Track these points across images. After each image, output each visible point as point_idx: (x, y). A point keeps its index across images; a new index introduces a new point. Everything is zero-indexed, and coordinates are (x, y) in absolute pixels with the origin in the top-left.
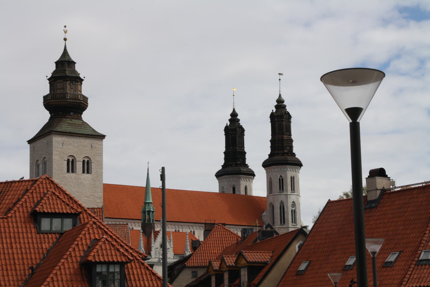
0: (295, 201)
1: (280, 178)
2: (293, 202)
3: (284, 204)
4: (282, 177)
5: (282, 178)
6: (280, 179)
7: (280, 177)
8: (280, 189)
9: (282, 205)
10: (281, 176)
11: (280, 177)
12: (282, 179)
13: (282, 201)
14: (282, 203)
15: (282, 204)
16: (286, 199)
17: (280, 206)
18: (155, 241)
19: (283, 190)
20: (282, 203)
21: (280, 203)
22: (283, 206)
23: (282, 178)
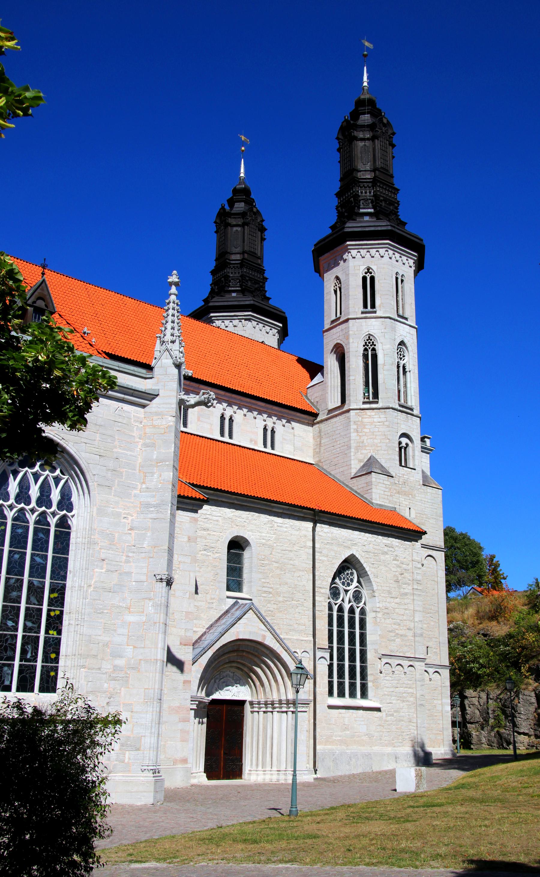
0: (406, 341)
1: (367, 275)
2: (399, 344)
3: (375, 345)
4: (371, 273)
5: (370, 275)
6: (364, 279)
7: (366, 273)
8: (365, 306)
9: (371, 347)
10: (368, 269)
11: (366, 273)
12: (372, 279)
13: (369, 337)
14: (369, 343)
15: (371, 346)
16: (383, 331)
17: (366, 350)
19: (373, 306)
20: (369, 343)
21: (366, 343)
22: (374, 350)
23: (370, 275)
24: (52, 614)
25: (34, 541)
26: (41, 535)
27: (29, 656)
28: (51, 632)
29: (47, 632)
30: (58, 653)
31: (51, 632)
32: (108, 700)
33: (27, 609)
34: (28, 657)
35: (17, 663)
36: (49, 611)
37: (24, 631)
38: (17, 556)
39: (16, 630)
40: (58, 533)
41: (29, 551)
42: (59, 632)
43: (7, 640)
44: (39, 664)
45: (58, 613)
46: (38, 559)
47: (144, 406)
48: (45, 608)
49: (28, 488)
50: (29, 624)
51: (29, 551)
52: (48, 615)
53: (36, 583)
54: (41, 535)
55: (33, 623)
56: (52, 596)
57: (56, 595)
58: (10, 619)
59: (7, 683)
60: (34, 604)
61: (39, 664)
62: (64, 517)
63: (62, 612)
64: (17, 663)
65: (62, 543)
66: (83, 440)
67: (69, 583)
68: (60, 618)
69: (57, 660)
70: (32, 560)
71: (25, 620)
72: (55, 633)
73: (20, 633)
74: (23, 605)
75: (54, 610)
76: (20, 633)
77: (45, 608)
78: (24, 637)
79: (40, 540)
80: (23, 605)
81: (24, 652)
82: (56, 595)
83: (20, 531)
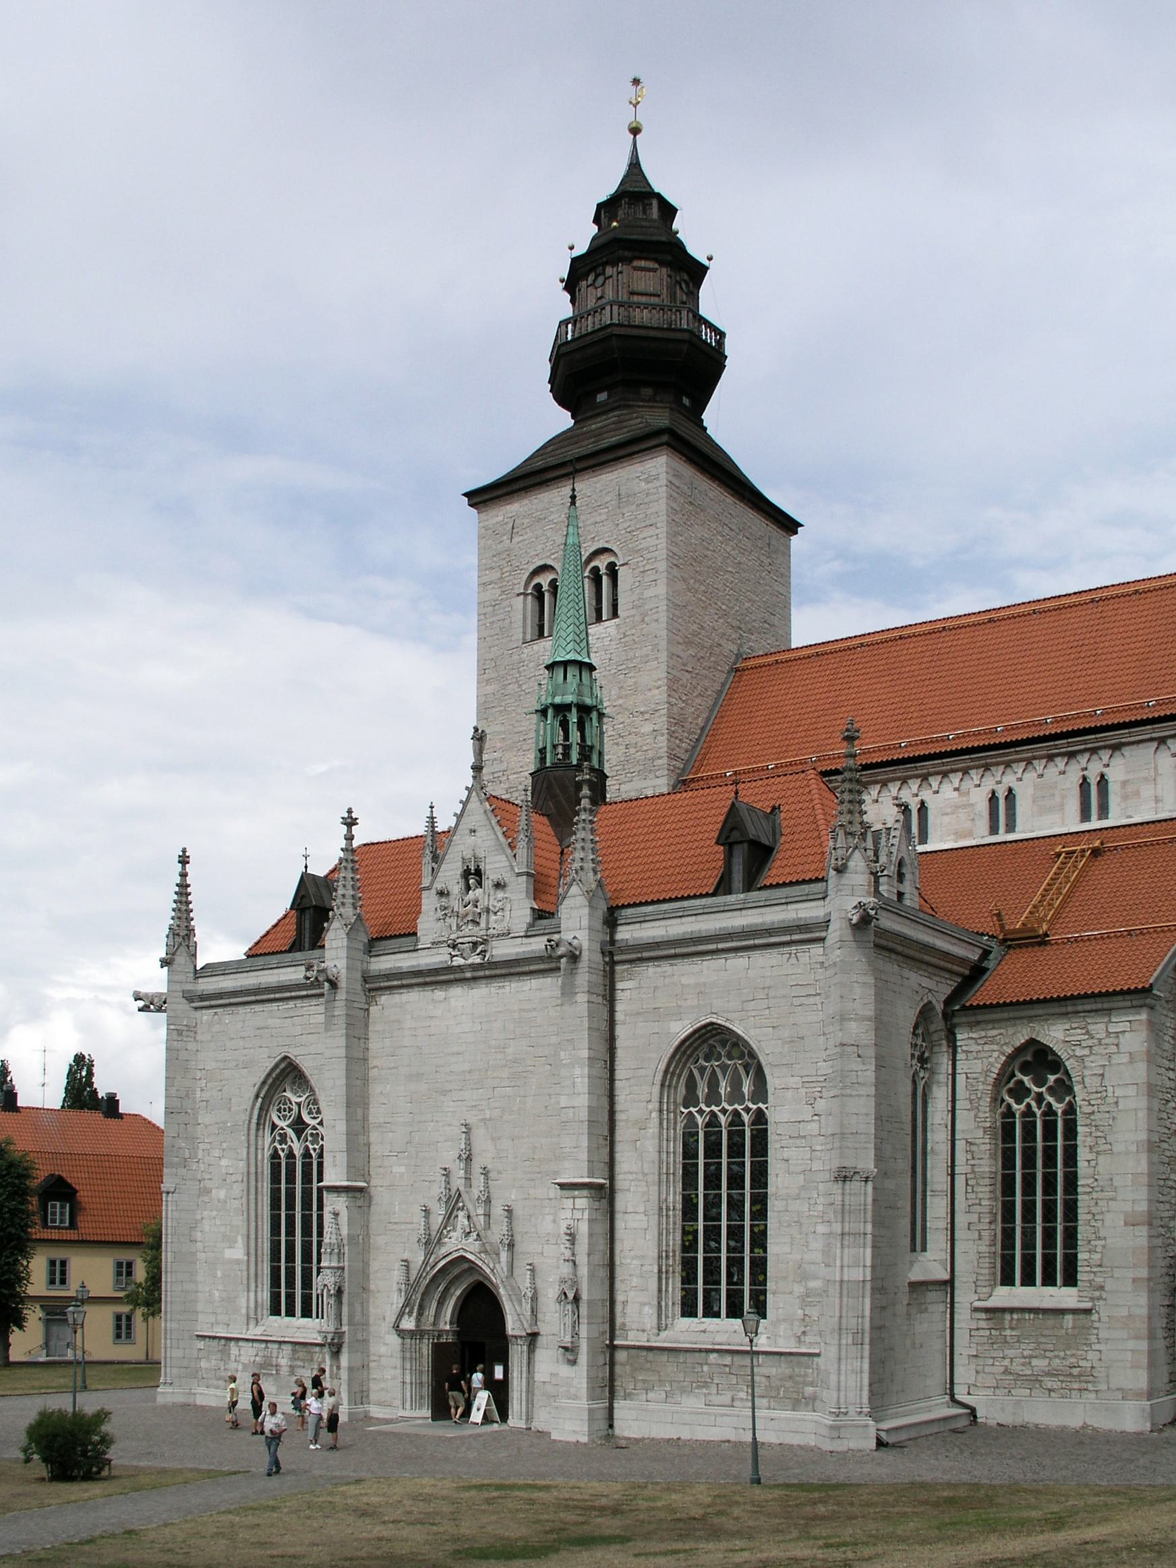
18: (435, 858)
24: (756, 1230)
25: (729, 1147)
26: (736, 1139)
27: (735, 1279)
28: (756, 1250)
29: (752, 1251)
30: (766, 1275)
31: (756, 1250)
32: (803, 1329)
33: (729, 1226)
34: (735, 1280)
35: (724, 1287)
36: (752, 1226)
37: (728, 1252)
38: (712, 1168)
39: (720, 1251)
40: (755, 1132)
41: (724, 1160)
42: (765, 1251)
43: (712, 1263)
44: (747, 1288)
45: (762, 1228)
46: (735, 1167)
47: (823, 939)
48: (747, 1223)
49: (718, 1085)
50: (732, 1243)
51: (724, 1160)
52: (752, 1231)
53: (735, 1196)
54: (736, 1139)
55: (737, 1242)
56: (754, 1209)
57: (758, 1207)
58: (713, 1240)
59: (716, 1309)
60: (736, 1220)
61: (747, 1288)
62: (760, 1113)
63: (766, 1225)
64: (724, 1287)
65: (760, 1144)
66: (749, 1014)
67: (771, 1190)
68: (764, 1233)
69: (764, 1282)
70: (729, 1169)
71: (728, 1239)
72: (761, 1251)
73: (724, 1255)
74: (724, 1223)
75: (758, 1225)
76: (724, 1255)
77: (747, 1223)
78: (728, 1258)
79: (735, 1144)
80: (724, 1223)
81: (730, 1275)
82: (758, 1207)
83: (713, 1138)
